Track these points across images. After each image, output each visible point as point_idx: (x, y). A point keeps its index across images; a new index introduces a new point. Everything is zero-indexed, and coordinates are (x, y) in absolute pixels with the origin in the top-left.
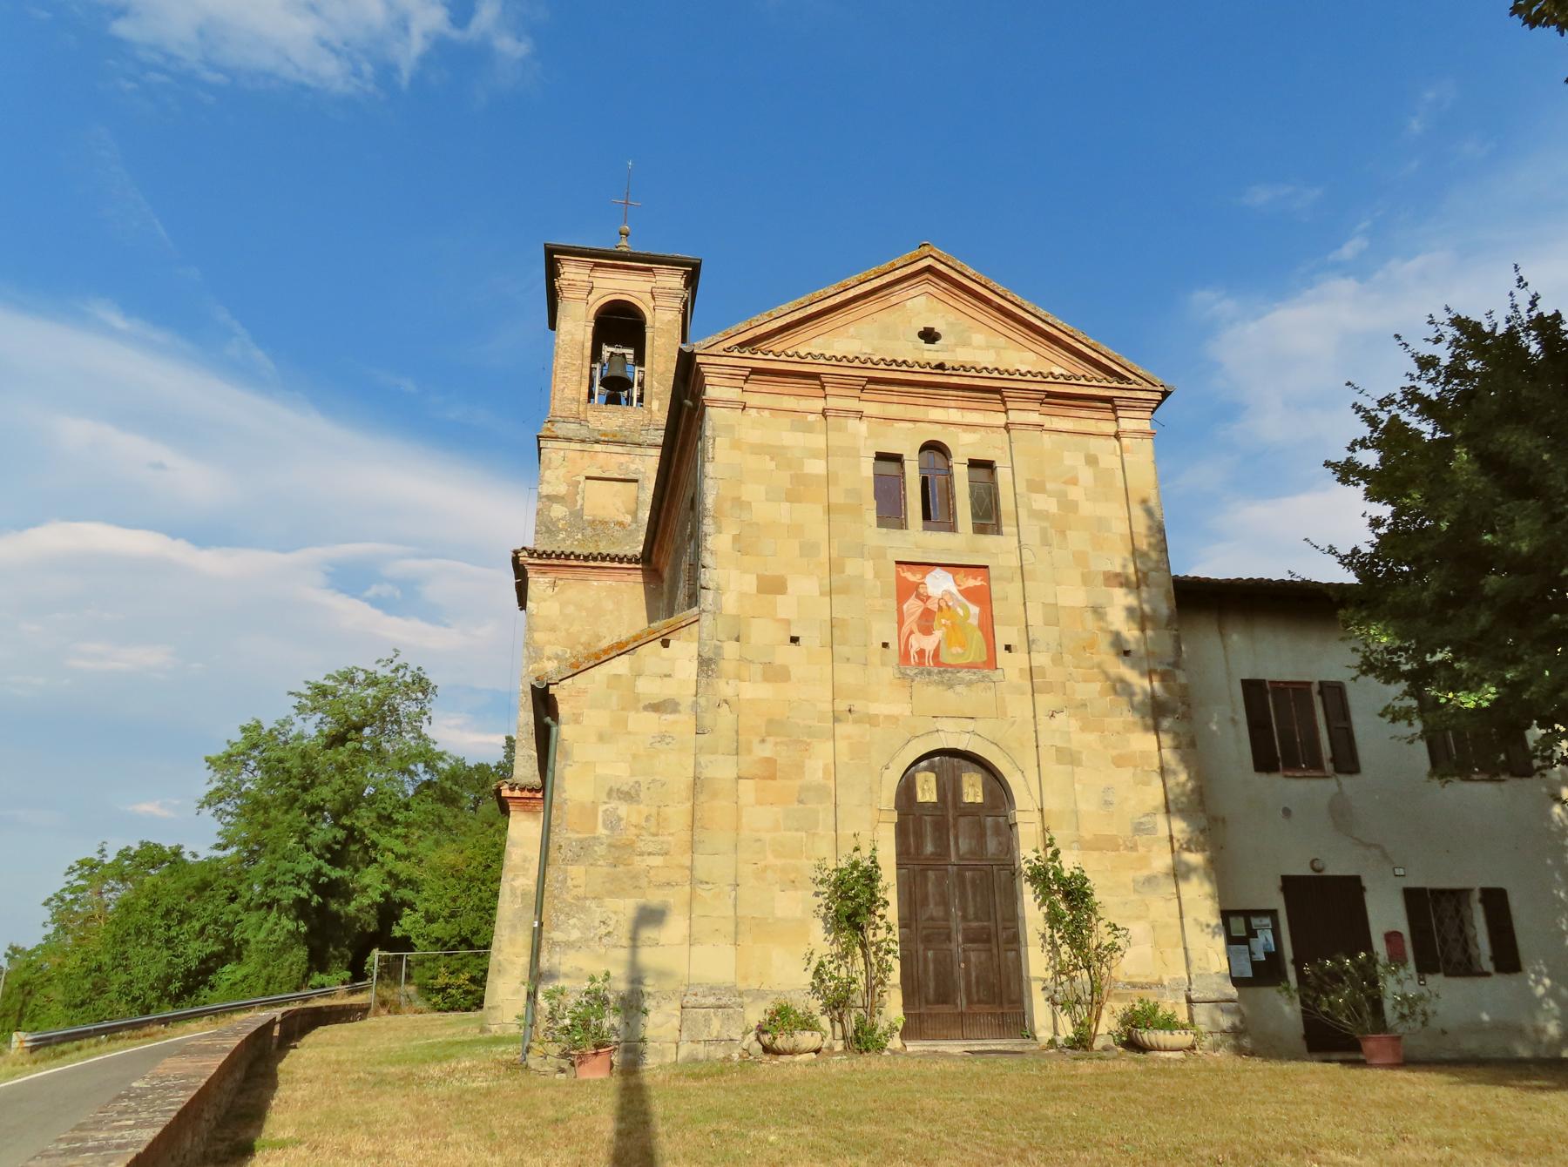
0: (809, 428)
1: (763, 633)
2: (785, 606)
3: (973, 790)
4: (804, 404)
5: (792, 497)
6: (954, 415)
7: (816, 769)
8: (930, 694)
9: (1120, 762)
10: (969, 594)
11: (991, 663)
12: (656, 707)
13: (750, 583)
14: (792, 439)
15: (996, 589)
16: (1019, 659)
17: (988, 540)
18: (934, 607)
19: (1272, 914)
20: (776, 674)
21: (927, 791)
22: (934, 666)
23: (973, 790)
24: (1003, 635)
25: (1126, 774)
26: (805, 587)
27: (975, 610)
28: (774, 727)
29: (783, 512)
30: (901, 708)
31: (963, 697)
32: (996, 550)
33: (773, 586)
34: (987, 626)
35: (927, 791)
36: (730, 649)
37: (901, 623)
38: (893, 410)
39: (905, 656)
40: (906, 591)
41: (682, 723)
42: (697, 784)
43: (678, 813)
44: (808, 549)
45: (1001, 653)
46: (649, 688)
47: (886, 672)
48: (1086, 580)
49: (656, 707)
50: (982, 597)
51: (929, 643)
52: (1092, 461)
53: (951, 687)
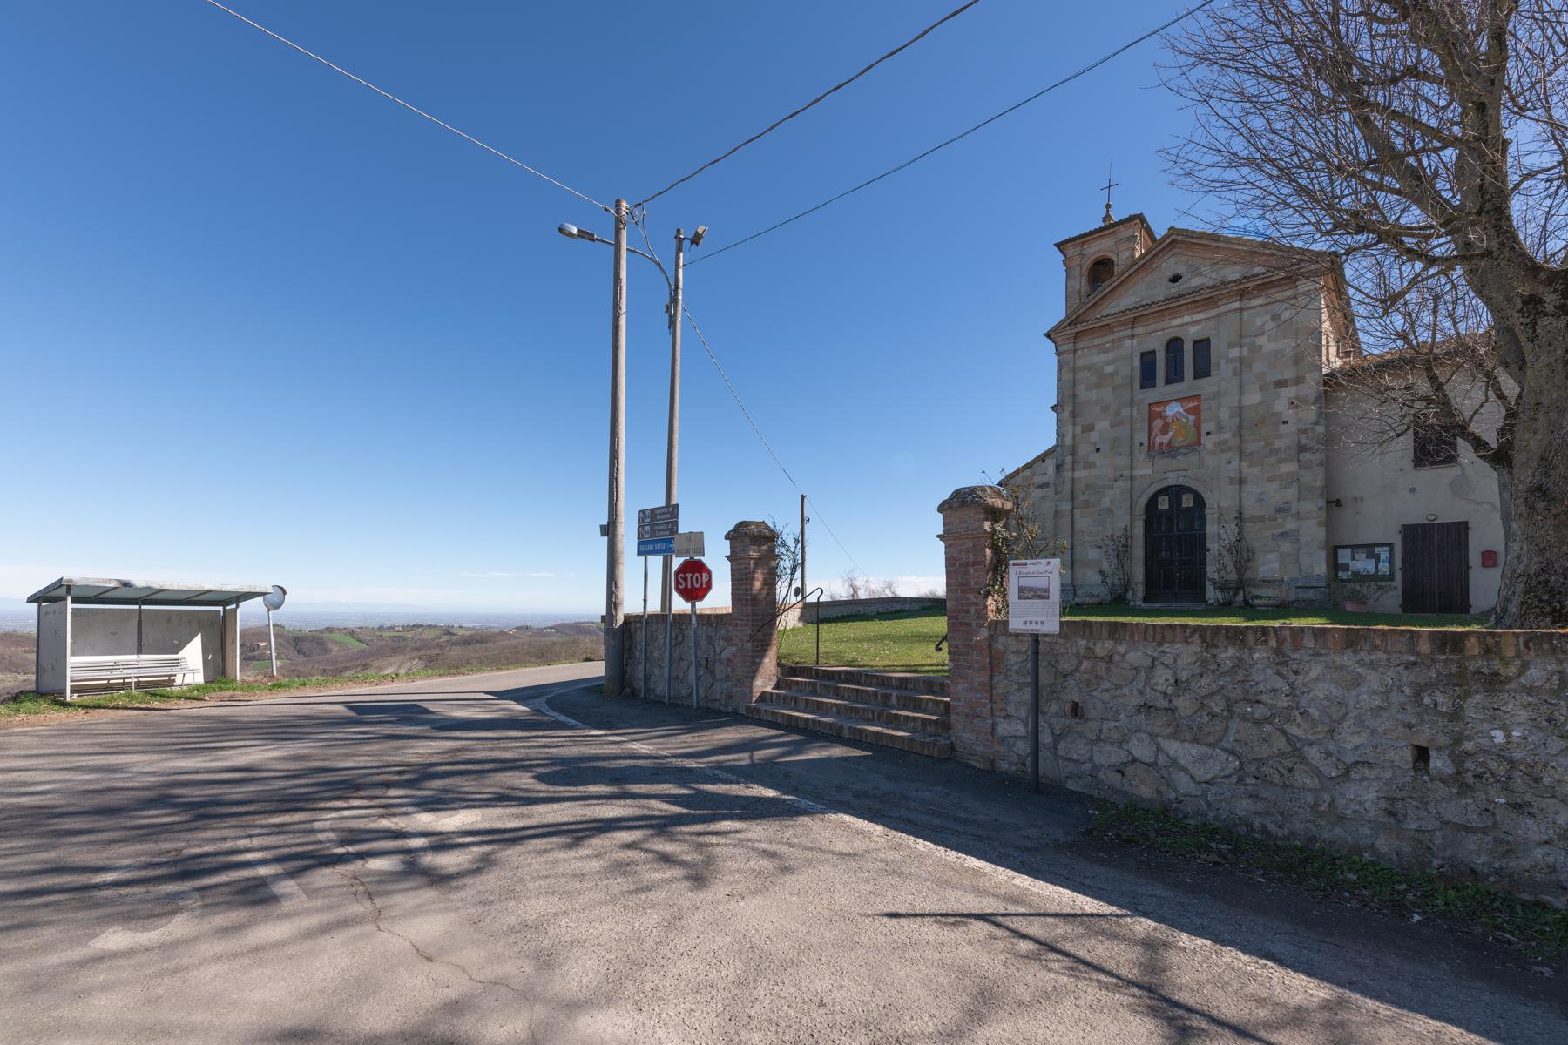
0: (1107, 351)
1: (1083, 450)
2: (1094, 436)
3: (1187, 501)
4: (1104, 340)
5: (1097, 386)
6: (1187, 319)
7: (1106, 502)
8: (1162, 463)
9: (1270, 480)
10: (1189, 411)
11: (1199, 443)
12: (1041, 486)
13: (1079, 429)
14: (1098, 359)
15: (1204, 405)
16: (1214, 438)
17: (1203, 382)
18: (1169, 420)
19: (1390, 545)
20: (1090, 465)
21: (1164, 504)
22: (1171, 451)
23: (1187, 501)
24: (1205, 428)
25: (1275, 485)
26: (1103, 425)
27: (1192, 418)
28: (1089, 487)
29: (1093, 395)
30: (1147, 471)
31: (1181, 462)
32: (1206, 386)
33: (1089, 428)
34: (1197, 425)
35: (1164, 504)
36: (1069, 459)
37: (1150, 433)
38: (1152, 327)
39: (1151, 447)
40: (1152, 417)
41: (1050, 491)
42: (1056, 513)
43: (1049, 524)
44: (1105, 409)
45: (1204, 438)
46: (1038, 480)
47: (1141, 457)
48: (1262, 388)
49: (1041, 486)
50: (1196, 411)
51: (1165, 439)
52: (1276, 317)
53: (1174, 457)
